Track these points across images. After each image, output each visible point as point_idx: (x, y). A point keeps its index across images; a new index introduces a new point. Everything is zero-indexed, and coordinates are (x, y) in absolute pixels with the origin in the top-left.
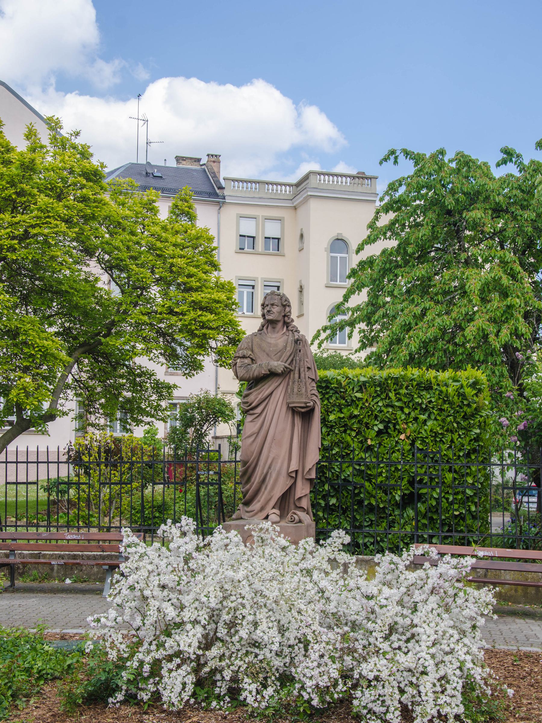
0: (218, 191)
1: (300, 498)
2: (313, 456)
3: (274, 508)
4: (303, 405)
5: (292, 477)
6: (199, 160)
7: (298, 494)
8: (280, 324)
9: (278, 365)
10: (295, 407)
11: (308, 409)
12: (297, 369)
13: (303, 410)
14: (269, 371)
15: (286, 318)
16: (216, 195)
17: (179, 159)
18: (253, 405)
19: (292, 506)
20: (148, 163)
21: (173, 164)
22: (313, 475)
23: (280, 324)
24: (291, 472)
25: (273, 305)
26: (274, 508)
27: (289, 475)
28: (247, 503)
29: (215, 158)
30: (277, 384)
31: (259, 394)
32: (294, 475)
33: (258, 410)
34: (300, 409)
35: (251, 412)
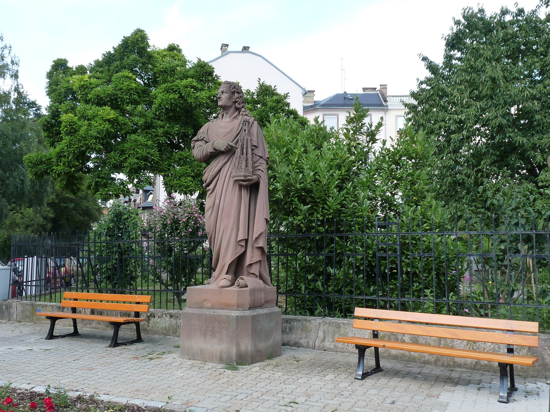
0: (384, 103)
1: (250, 265)
3: (227, 273)
4: (242, 178)
6: (375, 89)
7: (248, 260)
8: (232, 110)
9: (222, 145)
11: (251, 182)
13: (245, 183)
14: (215, 149)
16: (383, 105)
17: (364, 89)
19: (245, 272)
20: (345, 92)
21: (361, 92)
23: (232, 110)
26: (227, 273)
28: (214, 271)
29: (384, 87)
31: (210, 171)
32: (243, 243)
33: (211, 187)
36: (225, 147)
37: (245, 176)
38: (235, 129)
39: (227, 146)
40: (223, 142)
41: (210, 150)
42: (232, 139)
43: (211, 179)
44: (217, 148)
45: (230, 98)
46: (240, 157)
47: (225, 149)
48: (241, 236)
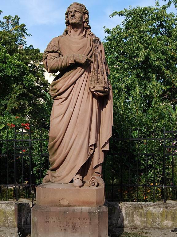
2: (106, 134)
4: (102, 90)
5: (92, 149)
10: (96, 91)
11: (105, 94)
12: (96, 61)
14: (75, 61)
15: (85, 24)
18: (60, 91)
22: (107, 148)
24: (91, 146)
25: (75, 11)
27: (89, 147)
30: (81, 73)
32: (93, 148)
33: (65, 95)
34: (99, 93)
35: (58, 97)
36: (85, 60)
37: (105, 88)
38: (88, 46)
39: (86, 60)
40: (83, 55)
41: (71, 61)
42: (87, 54)
43: (66, 88)
44: (77, 61)
45: (82, 18)
46: (98, 71)
47: (85, 62)
48: (92, 142)
